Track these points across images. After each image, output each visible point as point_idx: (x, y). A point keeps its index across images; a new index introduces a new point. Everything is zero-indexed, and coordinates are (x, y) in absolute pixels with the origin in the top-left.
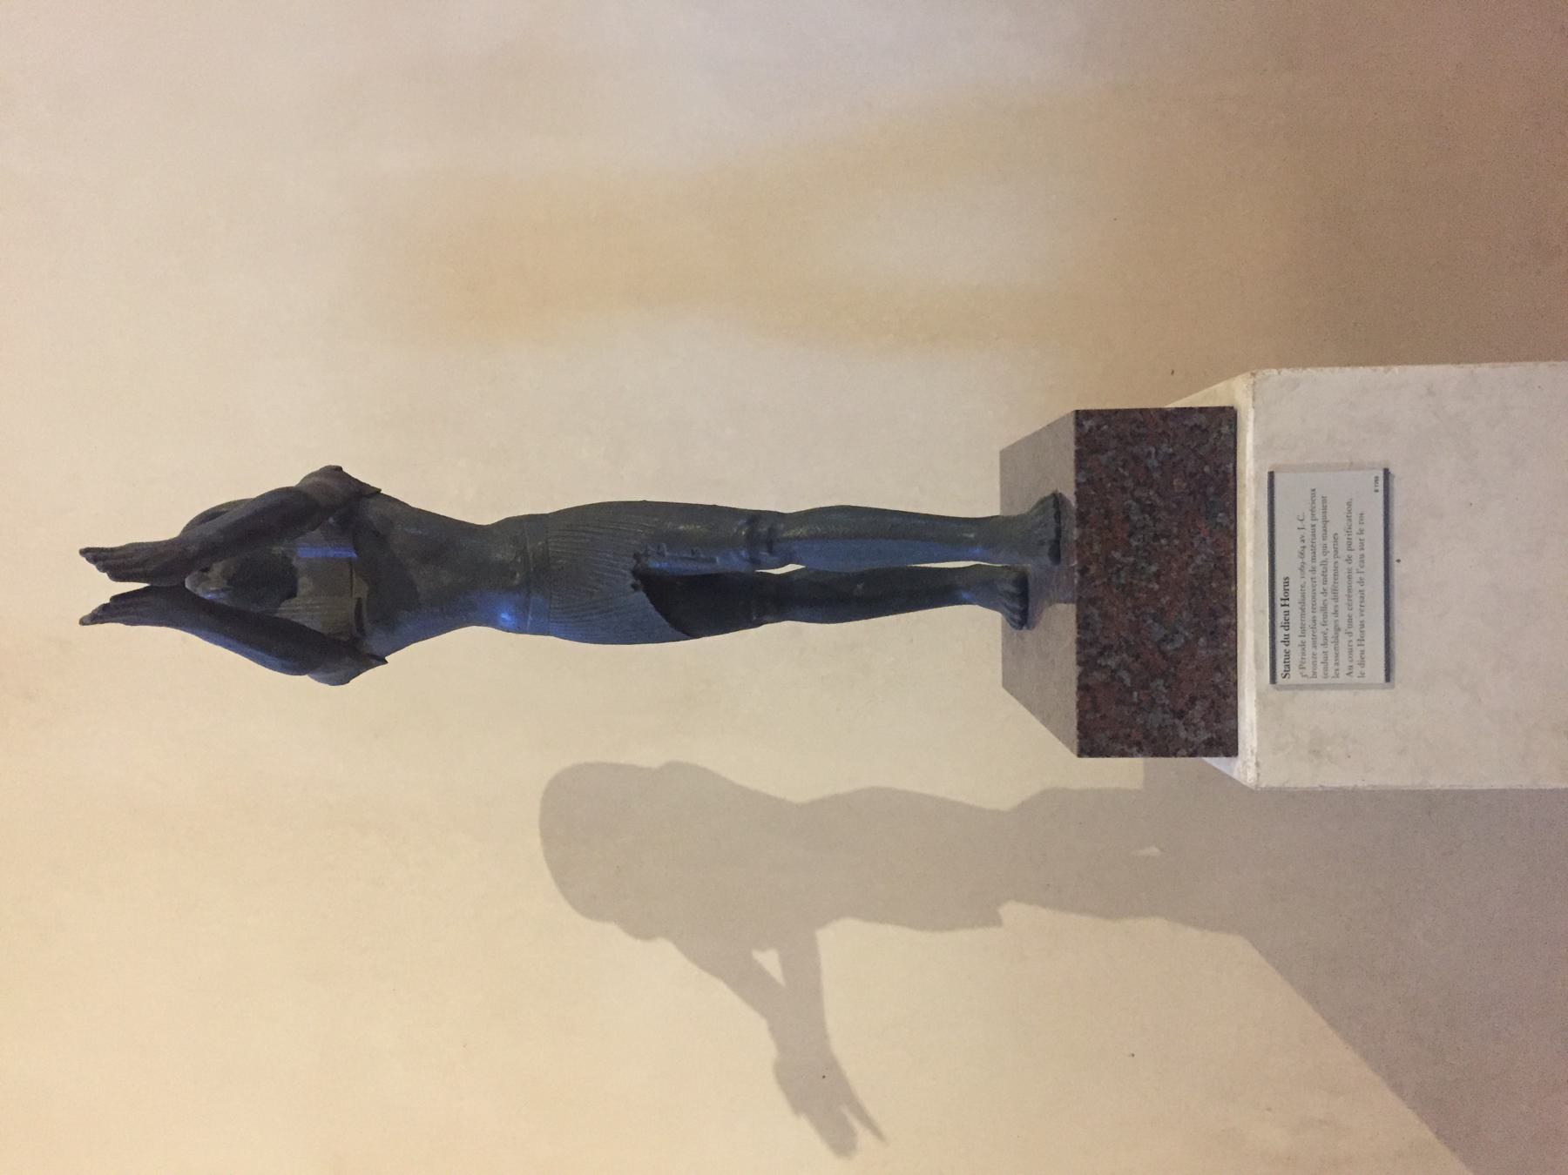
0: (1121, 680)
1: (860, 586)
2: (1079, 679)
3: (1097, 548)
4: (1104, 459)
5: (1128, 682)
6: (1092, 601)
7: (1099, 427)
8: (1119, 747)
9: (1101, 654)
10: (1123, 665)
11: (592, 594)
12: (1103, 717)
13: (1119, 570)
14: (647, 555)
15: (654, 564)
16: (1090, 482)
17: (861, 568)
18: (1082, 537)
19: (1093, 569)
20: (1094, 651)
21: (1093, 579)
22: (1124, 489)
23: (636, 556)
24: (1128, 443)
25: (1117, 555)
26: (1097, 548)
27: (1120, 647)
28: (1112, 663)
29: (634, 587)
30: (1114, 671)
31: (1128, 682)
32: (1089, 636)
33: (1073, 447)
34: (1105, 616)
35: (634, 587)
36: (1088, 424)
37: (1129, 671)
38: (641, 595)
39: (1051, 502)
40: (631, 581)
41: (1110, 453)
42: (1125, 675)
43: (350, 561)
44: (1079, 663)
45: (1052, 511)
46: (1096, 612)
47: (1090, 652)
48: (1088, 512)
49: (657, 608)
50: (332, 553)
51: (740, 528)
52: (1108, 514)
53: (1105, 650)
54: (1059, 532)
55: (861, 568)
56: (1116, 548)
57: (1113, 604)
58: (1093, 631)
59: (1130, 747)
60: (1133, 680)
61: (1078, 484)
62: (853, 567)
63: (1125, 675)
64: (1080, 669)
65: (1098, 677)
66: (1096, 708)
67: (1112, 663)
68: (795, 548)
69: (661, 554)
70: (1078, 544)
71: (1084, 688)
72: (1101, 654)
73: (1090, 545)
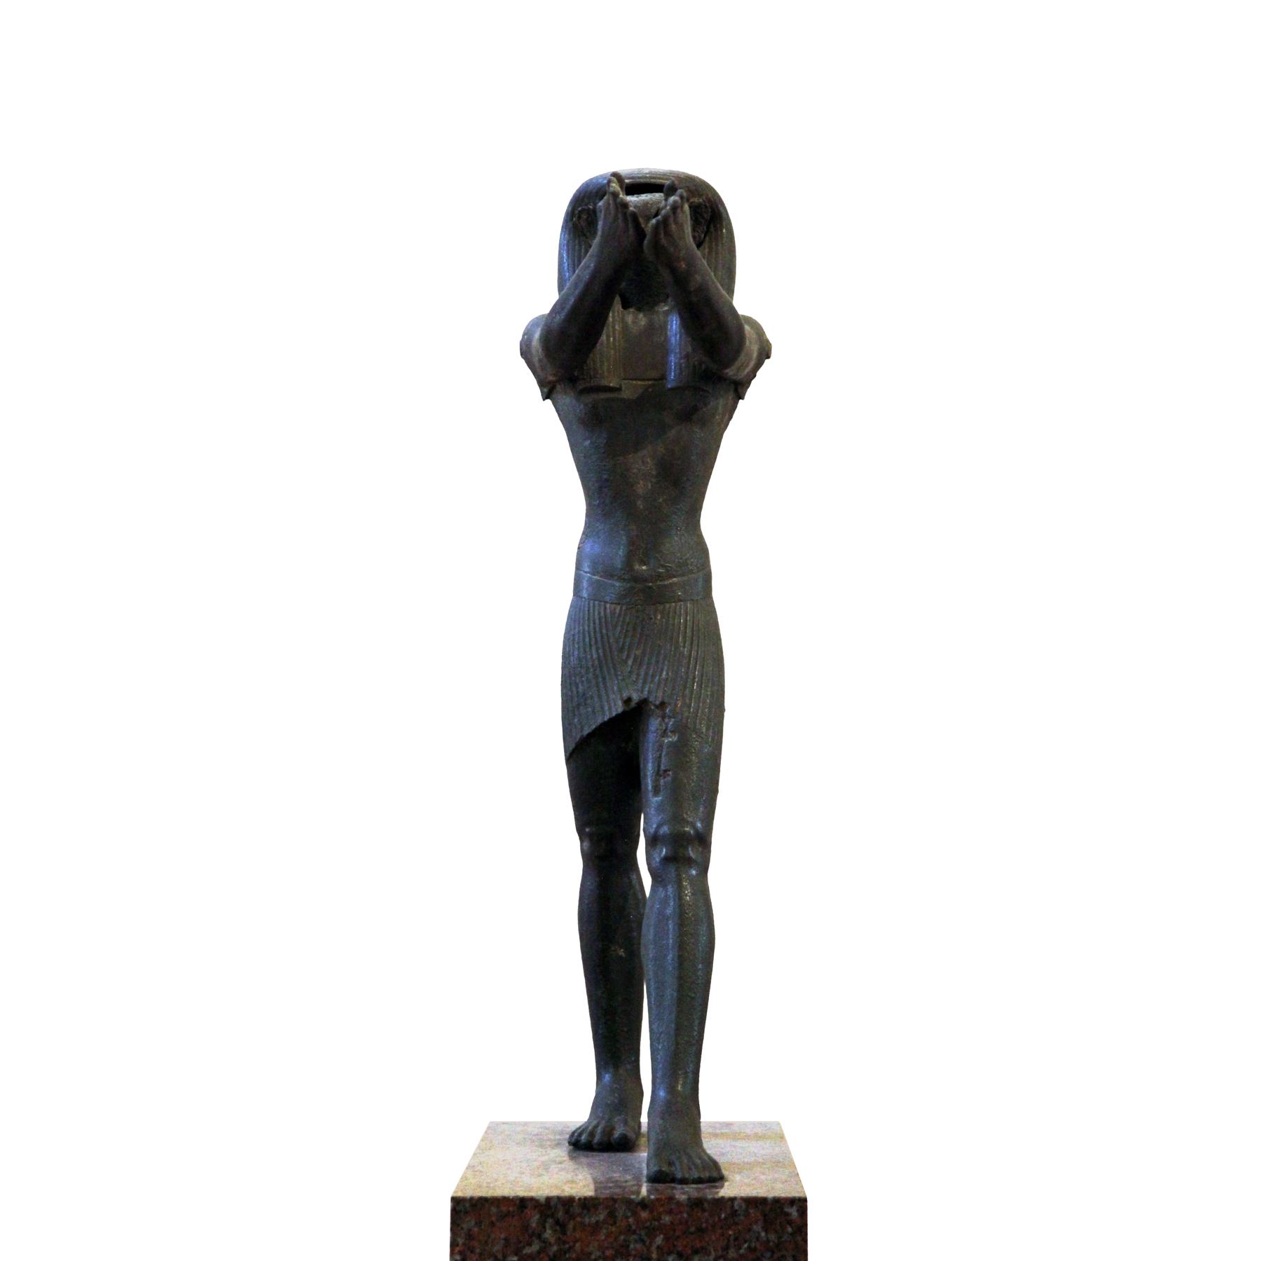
0: (530, 1244)
1: (621, 952)
2: (532, 1199)
3: (667, 1219)
5: (527, 1251)
6: (612, 1214)
7: (790, 1223)
8: (460, 1241)
9: (557, 1222)
10: (546, 1244)
11: (621, 650)
12: (493, 1224)
13: (643, 1241)
14: (663, 717)
15: (654, 724)
16: (734, 1213)
17: (642, 957)
18: (679, 1203)
19: (644, 1214)
20: (560, 1214)
21: (635, 1214)
22: (726, 1248)
23: (662, 705)
24: (773, 1252)
25: (659, 1240)
26: (667, 1219)
27: (564, 1243)
28: (548, 1234)
30: (539, 1236)
31: (527, 1251)
32: (576, 1209)
33: (771, 1195)
34: (596, 1227)
35: (628, 701)
36: (793, 1212)
37: (542, 1251)
38: (619, 708)
39: (715, 1175)
40: (636, 697)
41: (763, 1234)
42: (535, 1247)
43: (663, 377)
44: (548, 1199)
45: (706, 1175)
46: (602, 1217)
47: (557, 1210)
48: (704, 1210)
49: (604, 725)
50: (673, 359)
51: (694, 827)
52: (700, 1230)
53: (561, 1226)
54: (684, 1181)
55: (642, 957)
56: (667, 1239)
57: (608, 1236)
58: (580, 1215)
59: (460, 1253)
60: (530, 1256)
61: (733, 1200)
62: (648, 953)
63: (535, 1247)
64: (543, 1200)
65: (534, 1219)
66: (503, 1216)
67: (548, 1234)
68: (670, 889)
69: (664, 734)
70: (671, 1198)
71: (523, 1203)
72: (557, 1222)
73: (670, 1212)
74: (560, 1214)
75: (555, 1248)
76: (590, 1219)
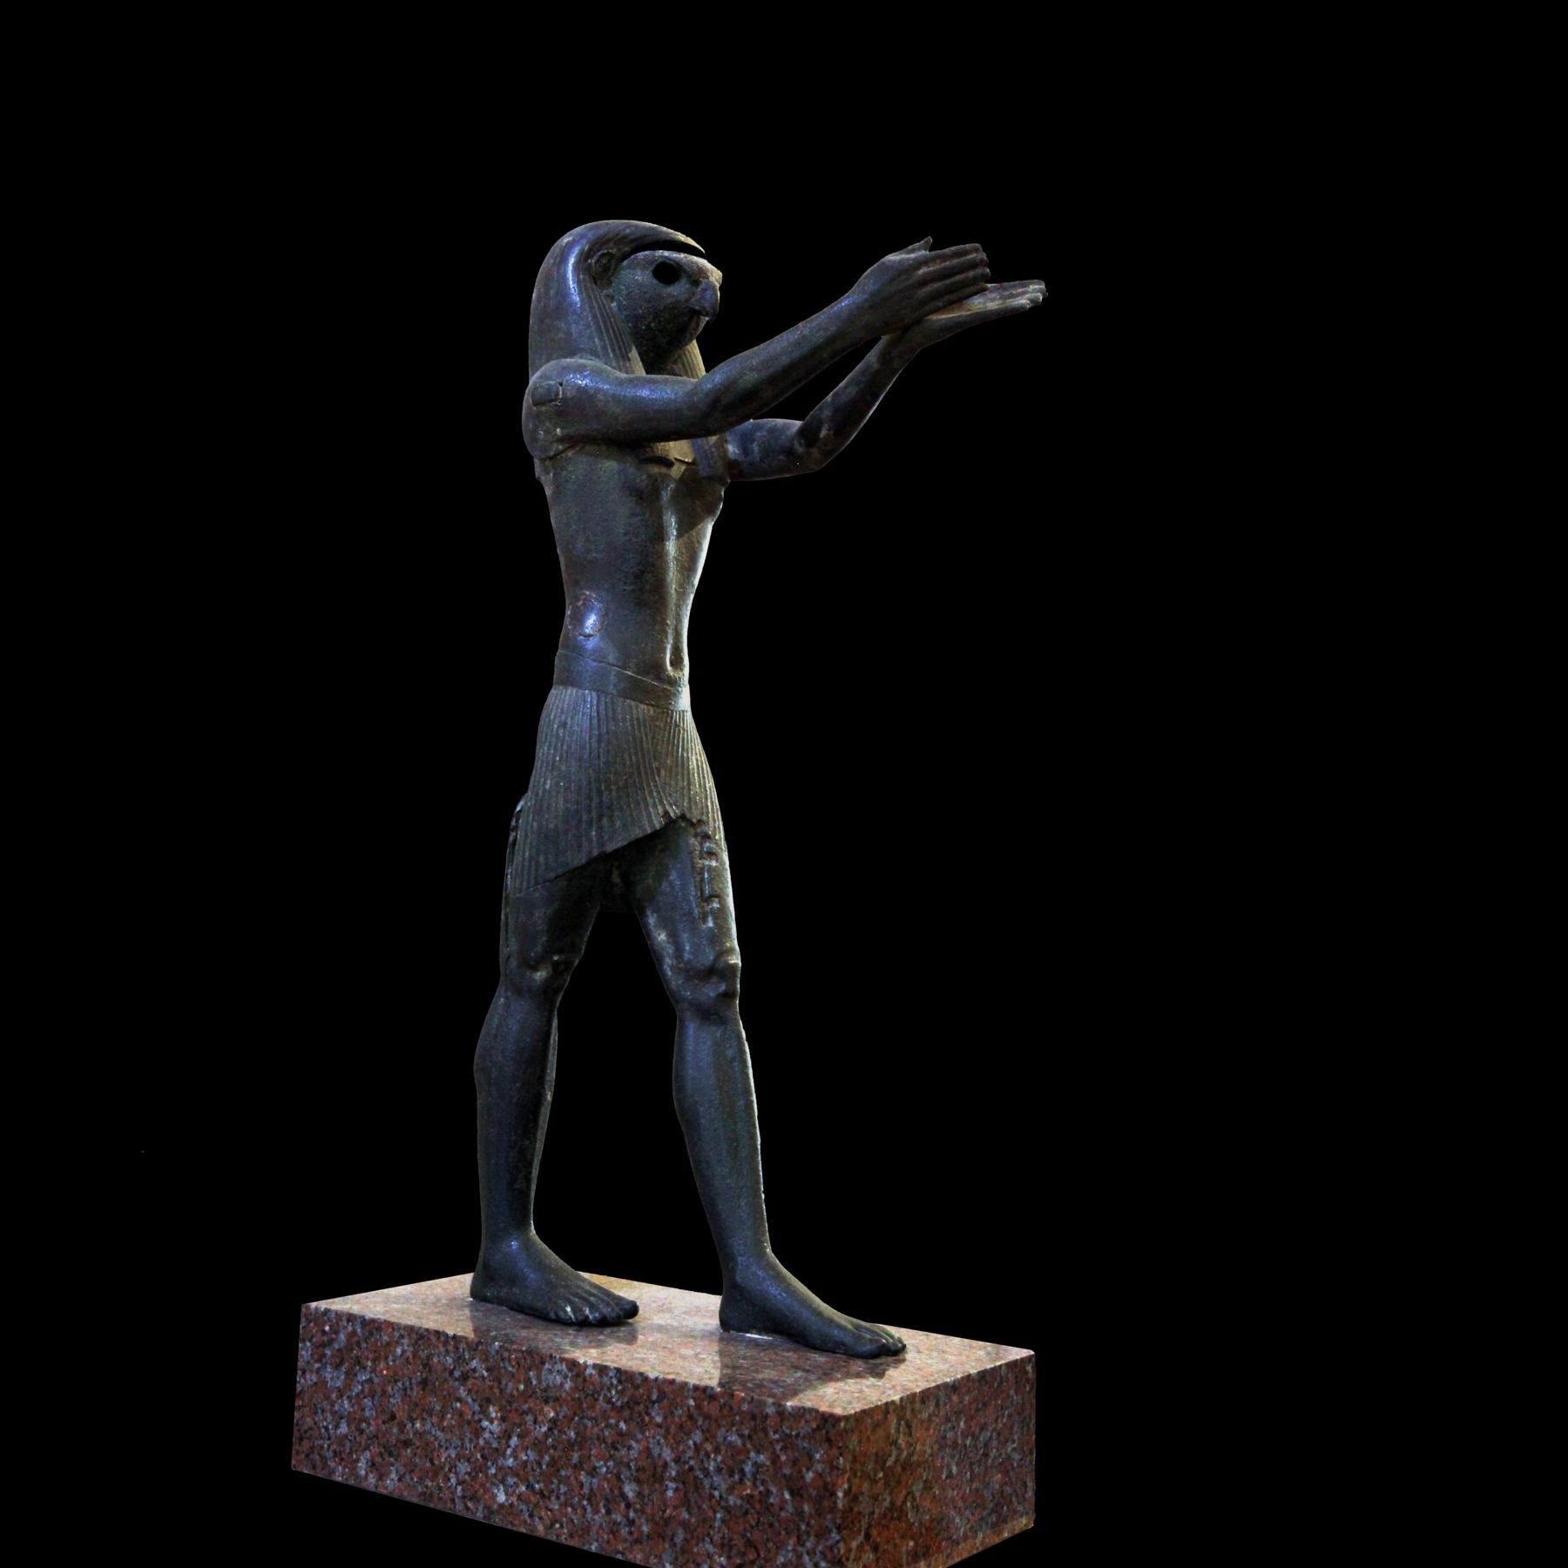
4: (1012, 1392)
19: (955, 1398)
29: (666, 813)
38: (658, 823)
76: (925, 1415)
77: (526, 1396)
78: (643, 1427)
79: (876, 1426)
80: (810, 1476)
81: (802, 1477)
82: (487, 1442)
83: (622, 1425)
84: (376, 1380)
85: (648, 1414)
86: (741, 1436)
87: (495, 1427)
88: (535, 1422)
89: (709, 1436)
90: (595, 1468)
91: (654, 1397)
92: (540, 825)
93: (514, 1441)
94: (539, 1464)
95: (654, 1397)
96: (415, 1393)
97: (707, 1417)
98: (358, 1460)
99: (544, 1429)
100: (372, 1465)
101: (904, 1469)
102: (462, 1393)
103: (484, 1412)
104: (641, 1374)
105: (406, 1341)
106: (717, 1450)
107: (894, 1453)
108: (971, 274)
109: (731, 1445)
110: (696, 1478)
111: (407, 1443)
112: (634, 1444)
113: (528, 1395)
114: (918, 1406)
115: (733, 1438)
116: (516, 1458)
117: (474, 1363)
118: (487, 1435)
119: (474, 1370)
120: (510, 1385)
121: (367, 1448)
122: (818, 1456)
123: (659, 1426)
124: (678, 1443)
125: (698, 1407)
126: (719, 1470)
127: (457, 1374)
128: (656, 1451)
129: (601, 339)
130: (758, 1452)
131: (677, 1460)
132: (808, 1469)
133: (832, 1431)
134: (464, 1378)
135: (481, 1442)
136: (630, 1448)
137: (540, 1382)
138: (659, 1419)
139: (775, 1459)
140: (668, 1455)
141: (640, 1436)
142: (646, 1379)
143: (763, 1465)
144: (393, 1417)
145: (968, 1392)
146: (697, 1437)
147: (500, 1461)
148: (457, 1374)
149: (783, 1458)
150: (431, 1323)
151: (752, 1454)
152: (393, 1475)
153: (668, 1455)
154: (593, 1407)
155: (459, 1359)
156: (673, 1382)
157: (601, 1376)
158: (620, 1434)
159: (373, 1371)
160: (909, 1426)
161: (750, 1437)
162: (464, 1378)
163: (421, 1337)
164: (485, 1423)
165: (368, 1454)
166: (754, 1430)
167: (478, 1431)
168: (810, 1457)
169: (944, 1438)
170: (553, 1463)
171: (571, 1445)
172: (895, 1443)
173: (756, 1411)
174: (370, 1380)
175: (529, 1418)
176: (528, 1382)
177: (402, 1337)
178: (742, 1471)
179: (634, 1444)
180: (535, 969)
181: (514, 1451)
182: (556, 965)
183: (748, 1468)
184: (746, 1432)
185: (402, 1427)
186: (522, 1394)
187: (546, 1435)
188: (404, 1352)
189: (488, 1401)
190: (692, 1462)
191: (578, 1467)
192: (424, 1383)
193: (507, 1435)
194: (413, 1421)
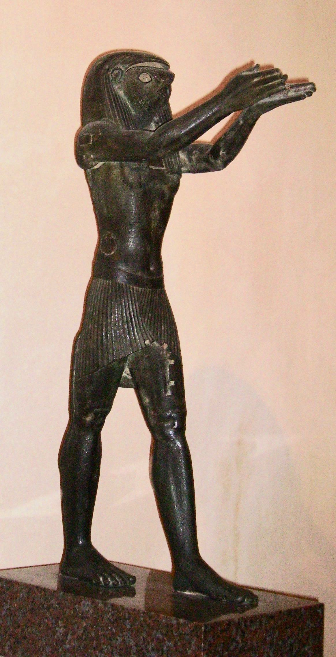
20: (243, 626)
74: (243, 626)
75: (241, 645)
77: (75, 616)
78: (122, 630)
79: (223, 631)
80: (190, 652)
81: (187, 652)
82: (58, 637)
83: (114, 629)
84: (12, 609)
85: (125, 625)
86: (162, 634)
87: (61, 630)
88: (78, 628)
89: (149, 634)
90: (103, 649)
91: (127, 617)
92: (87, 347)
93: (69, 637)
94: (79, 647)
95: (127, 617)
96: (28, 615)
97: (149, 625)
98: (5, 646)
99: (82, 631)
100: (11, 647)
101: (240, 652)
102: (48, 615)
103: (57, 623)
104: (121, 606)
105: (24, 591)
106: (152, 640)
107: (234, 644)
108: (276, 82)
109: (158, 639)
110: (143, 653)
111: (25, 638)
112: (118, 638)
113: (75, 616)
114: (248, 623)
115: (159, 635)
116: (70, 645)
117: (53, 601)
118: (58, 634)
119: (53, 604)
120: (68, 612)
121: (8, 640)
122: (193, 643)
123: (129, 630)
124: (136, 637)
125: (145, 621)
126: (153, 650)
127: (45, 606)
128: (127, 641)
129: (114, 111)
130: (169, 641)
131: (136, 645)
132: (189, 649)
133: (199, 632)
134: (48, 608)
135: (56, 637)
136: (117, 640)
137: (79, 609)
138: (128, 627)
139: (176, 645)
140: (132, 643)
141: (120, 634)
142: (123, 608)
143: (171, 647)
144: (19, 626)
145: (281, 619)
146: (144, 635)
147: (64, 646)
148: (45, 606)
149: (179, 644)
150: (36, 581)
151: (167, 642)
152: (19, 652)
153: (132, 643)
154: (101, 621)
155: (47, 599)
156: (134, 610)
157: (105, 607)
158: (113, 634)
159: (11, 605)
160: (243, 632)
161: (166, 635)
162: (48, 608)
163: (30, 589)
164: (57, 629)
165: (9, 643)
166: (168, 631)
167: (54, 633)
168: (190, 643)
169: (265, 639)
170: (85, 647)
171: (92, 639)
172: (235, 639)
173: (169, 623)
174: (9, 609)
175: (76, 626)
176: (75, 609)
177: (22, 589)
178: (162, 650)
179: (118, 638)
180: (86, 415)
181: (69, 641)
182: (96, 414)
183: (165, 648)
184: (164, 632)
185: (23, 630)
186: (72, 615)
187: (82, 634)
188: (23, 596)
189: (58, 618)
190: (142, 646)
191: (95, 648)
192: (32, 610)
193: (66, 634)
194: (27, 627)
